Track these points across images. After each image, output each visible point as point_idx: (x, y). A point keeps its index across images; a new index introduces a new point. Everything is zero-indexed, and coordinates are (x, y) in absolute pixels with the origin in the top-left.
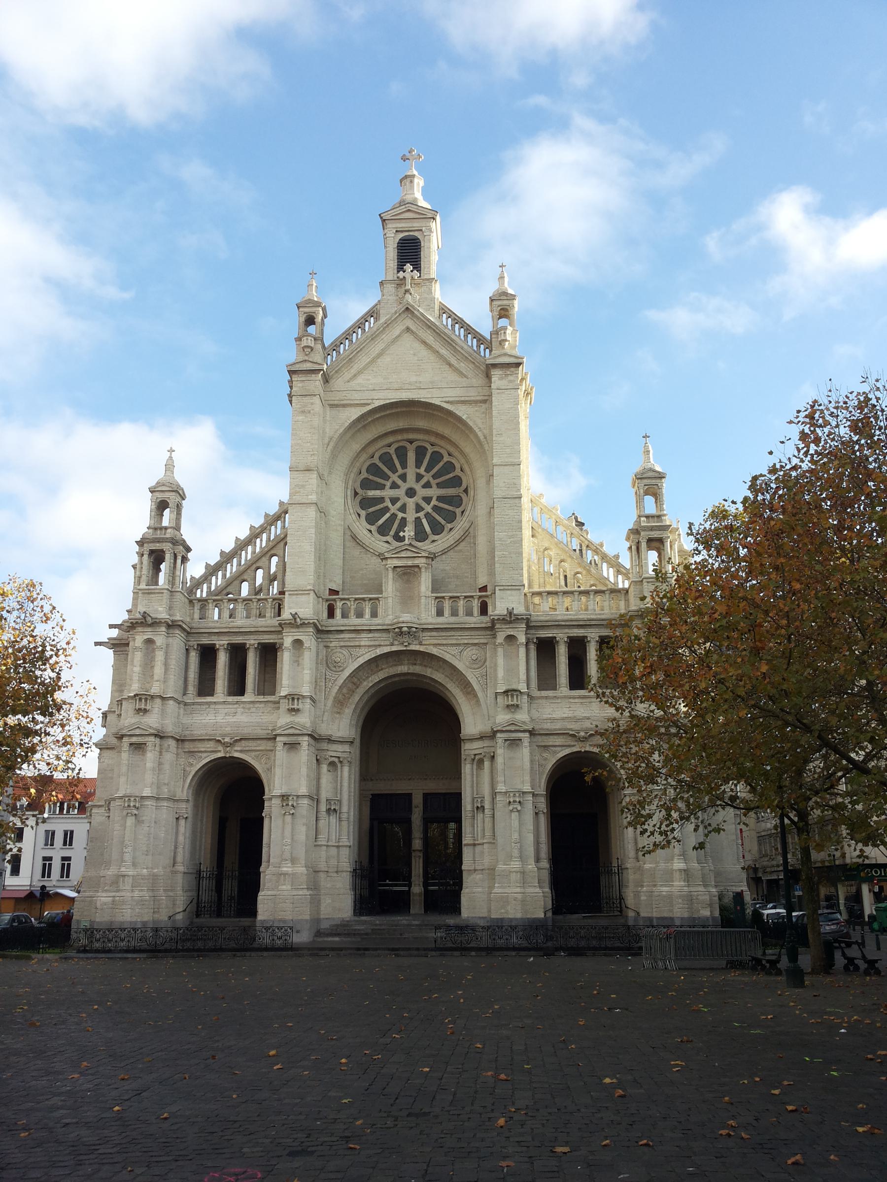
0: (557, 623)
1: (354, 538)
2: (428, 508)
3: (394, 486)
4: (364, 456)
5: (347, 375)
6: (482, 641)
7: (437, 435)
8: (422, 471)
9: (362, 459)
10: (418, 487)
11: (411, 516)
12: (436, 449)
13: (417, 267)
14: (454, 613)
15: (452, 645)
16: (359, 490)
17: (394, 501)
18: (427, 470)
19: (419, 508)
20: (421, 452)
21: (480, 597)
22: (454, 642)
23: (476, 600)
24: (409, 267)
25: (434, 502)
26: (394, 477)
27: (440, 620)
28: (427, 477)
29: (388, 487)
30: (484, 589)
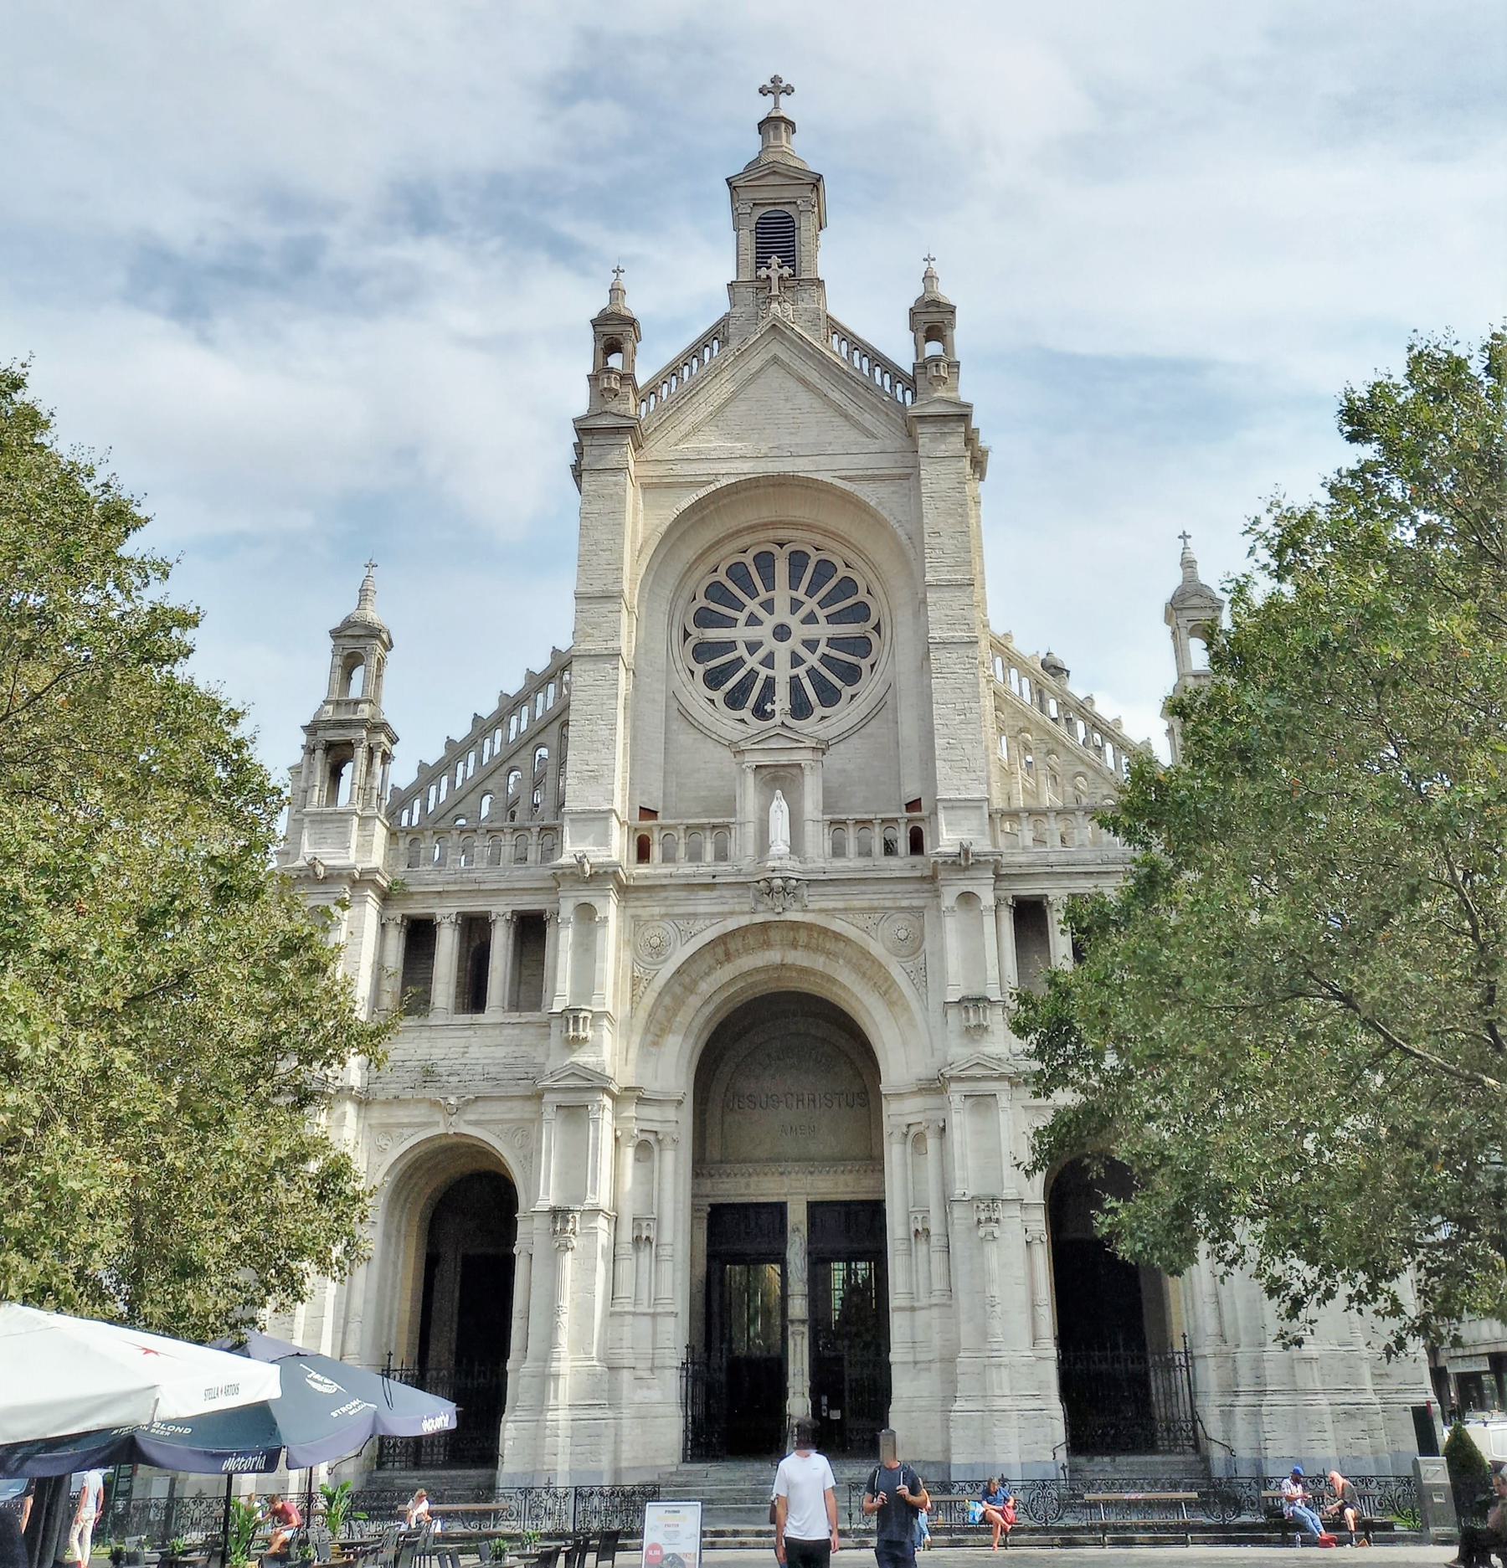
0: (1049, 869)
1: (684, 714)
2: (812, 660)
3: (753, 621)
4: (703, 568)
5: (674, 436)
6: (916, 903)
7: (826, 533)
8: (800, 594)
9: (697, 575)
10: (793, 622)
11: (782, 673)
12: (824, 556)
13: (789, 259)
14: (865, 852)
15: (863, 910)
16: (692, 629)
17: (753, 647)
18: (810, 593)
19: (796, 661)
20: (798, 561)
21: (910, 820)
22: (865, 904)
23: (903, 827)
24: (775, 260)
25: (823, 648)
26: (752, 605)
27: (839, 863)
28: (811, 604)
29: (741, 623)
30: (914, 805)
